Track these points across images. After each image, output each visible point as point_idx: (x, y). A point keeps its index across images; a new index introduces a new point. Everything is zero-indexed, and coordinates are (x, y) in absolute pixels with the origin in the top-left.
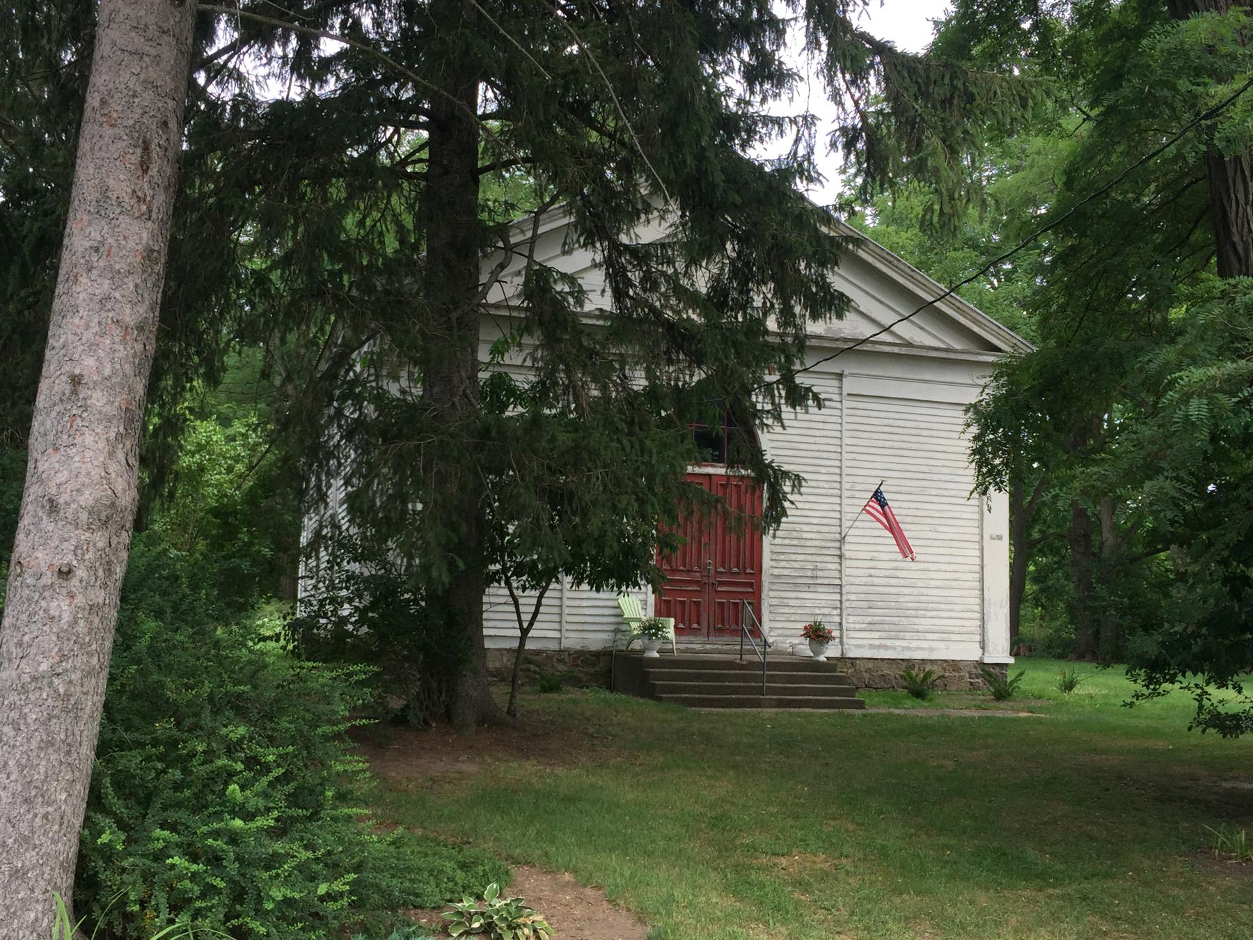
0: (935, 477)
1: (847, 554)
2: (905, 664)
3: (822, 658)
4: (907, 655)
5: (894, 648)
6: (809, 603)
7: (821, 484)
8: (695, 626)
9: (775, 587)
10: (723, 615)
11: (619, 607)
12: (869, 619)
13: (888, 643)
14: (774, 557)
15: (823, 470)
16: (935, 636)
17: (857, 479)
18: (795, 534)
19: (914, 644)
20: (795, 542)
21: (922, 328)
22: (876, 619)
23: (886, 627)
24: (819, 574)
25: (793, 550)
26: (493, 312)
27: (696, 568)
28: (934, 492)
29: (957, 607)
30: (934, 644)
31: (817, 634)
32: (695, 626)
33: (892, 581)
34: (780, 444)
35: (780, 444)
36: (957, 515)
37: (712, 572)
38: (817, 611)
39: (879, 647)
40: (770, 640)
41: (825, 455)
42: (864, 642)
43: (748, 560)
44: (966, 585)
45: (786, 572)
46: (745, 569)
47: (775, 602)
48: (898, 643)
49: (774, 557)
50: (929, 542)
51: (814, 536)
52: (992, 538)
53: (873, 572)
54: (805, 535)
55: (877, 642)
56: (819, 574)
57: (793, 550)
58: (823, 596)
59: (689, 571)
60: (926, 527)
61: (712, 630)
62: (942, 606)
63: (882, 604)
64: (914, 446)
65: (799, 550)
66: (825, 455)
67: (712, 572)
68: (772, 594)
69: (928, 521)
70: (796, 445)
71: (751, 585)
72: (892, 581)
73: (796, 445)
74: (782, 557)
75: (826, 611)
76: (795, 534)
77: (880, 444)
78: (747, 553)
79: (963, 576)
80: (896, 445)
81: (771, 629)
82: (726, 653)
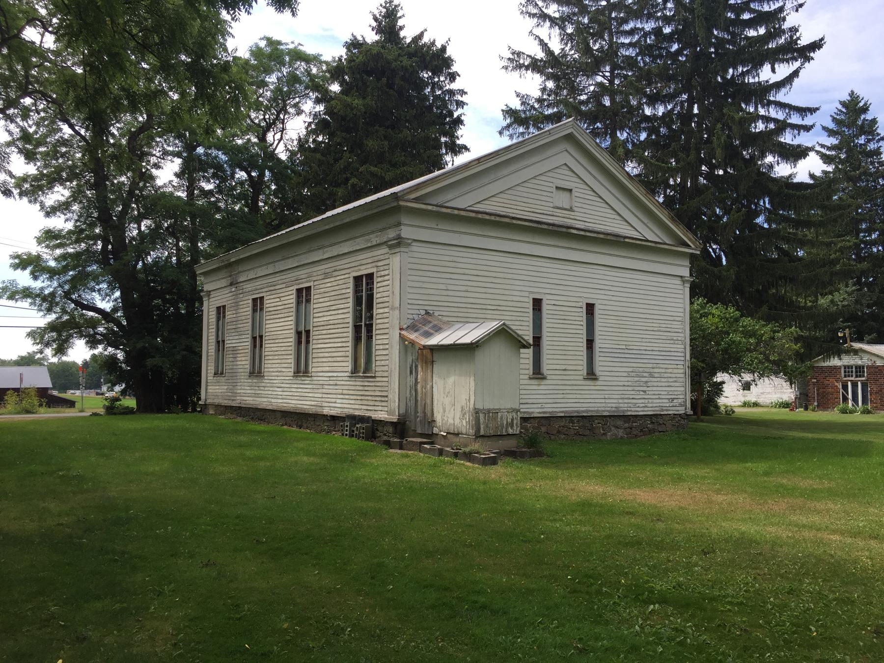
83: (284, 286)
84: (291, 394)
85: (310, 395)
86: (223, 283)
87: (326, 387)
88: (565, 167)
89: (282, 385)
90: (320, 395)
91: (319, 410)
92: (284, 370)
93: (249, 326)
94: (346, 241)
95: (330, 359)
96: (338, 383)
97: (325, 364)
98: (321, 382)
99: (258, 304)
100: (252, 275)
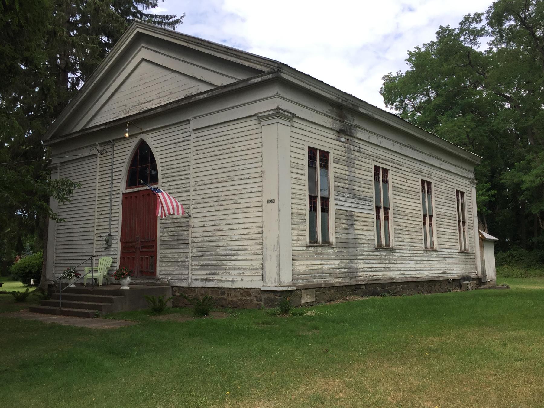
0: (237, 168)
1: (192, 224)
2: (220, 291)
4: (220, 285)
5: (213, 280)
7: (182, 186)
12: (202, 263)
13: (210, 277)
15: (183, 177)
16: (235, 272)
17: (198, 179)
19: (224, 278)
21: (227, 76)
22: (205, 262)
23: (210, 267)
24: (180, 238)
26: (69, 137)
28: (236, 178)
29: (248, 252)
30: (235, 278)
33: (214, 238)
36: (249, 190)
38: (179, 260)
39: (207, 280)
41: (183, 169)
42: (199, 277)
44: (254, 236)
47: (162, 255)
48: (216, 277)
50: (233, 211)
52: (268, 202)
53: (204, 234)
55: (205, 277)
56: (180, 238)
58: (182, 251)
60: (232, 202)
62: (240, 252)
63: (208, 253)
64: (225, 151)
66: (183, 169)
68: (161, 251)
69: (233, 197)
72: (214, 238)
75: (183, 259)
77: (208, 155)
79: (252, 231)
80: (216, 153)
81: (161, 271)
82: (144, 284)
83: (409, 170)
84: (423, 266)
85: (438, 266)
86: (329, 122)
87: (447, 259)
88: (144, 64)
89: (415, 258)
90: (444, 266)
91: (469, 275)
92: (415, 245)
93: (372, 192)
94: (452, 164)
95: (448, 240)
96: (454, 256)
97: (445, 243)
98: (444, 256)
99: (381, 174)
100: (374, 139)
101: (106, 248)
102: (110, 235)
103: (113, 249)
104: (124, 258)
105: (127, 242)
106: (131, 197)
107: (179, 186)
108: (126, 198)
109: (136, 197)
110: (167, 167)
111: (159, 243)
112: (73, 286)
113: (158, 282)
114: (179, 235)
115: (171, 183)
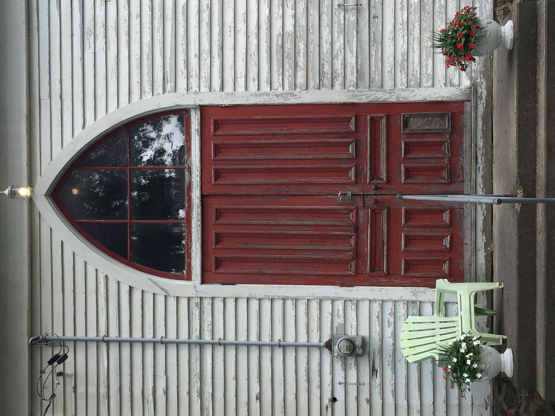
3: (508, 29)
6: (402, 16)
8: (446, 217)
9: (377, 78)
10: (427, 169)
11: (420, 363)
14: (327, 81)
18: (288, 46)
20: (301, 46)
25: (314, 48)
27: (352, 216)
31: (461, 40)
32: (446, 217)
34: (146, 78)
35: (146, 78)
37: (357, 190)
40: (466, 83)
43: (336, 129)
45: (351, 60)
46: (348, 134)
47: (401, 78)
49: (327, 81)
51: (289, 12)
54: (289, 27)
57: (314, 48)
59: (357, 229)
61: (452, 188)
65: (314, 37)
67: (357, 190)
68: (388, 84)
70: (146, 50)
71: (375, 122)
73: (146, 50)
74: (327, 68)
76: (288, 46)
78: (323, 130)
81: (448, 83)
101: (373, 371)
102: (329, 345)
103: (376, 328)
104: (409, 266)
105: (358, 254)
106: (219, 238)
107: (205, 16)
108: (219, 263)
109: (219, 214)
110: (145, 71)
111: (366, 96)
112: (508, 356)
113: (483, 91)
114: (343, 7)
115: (194, 50)
